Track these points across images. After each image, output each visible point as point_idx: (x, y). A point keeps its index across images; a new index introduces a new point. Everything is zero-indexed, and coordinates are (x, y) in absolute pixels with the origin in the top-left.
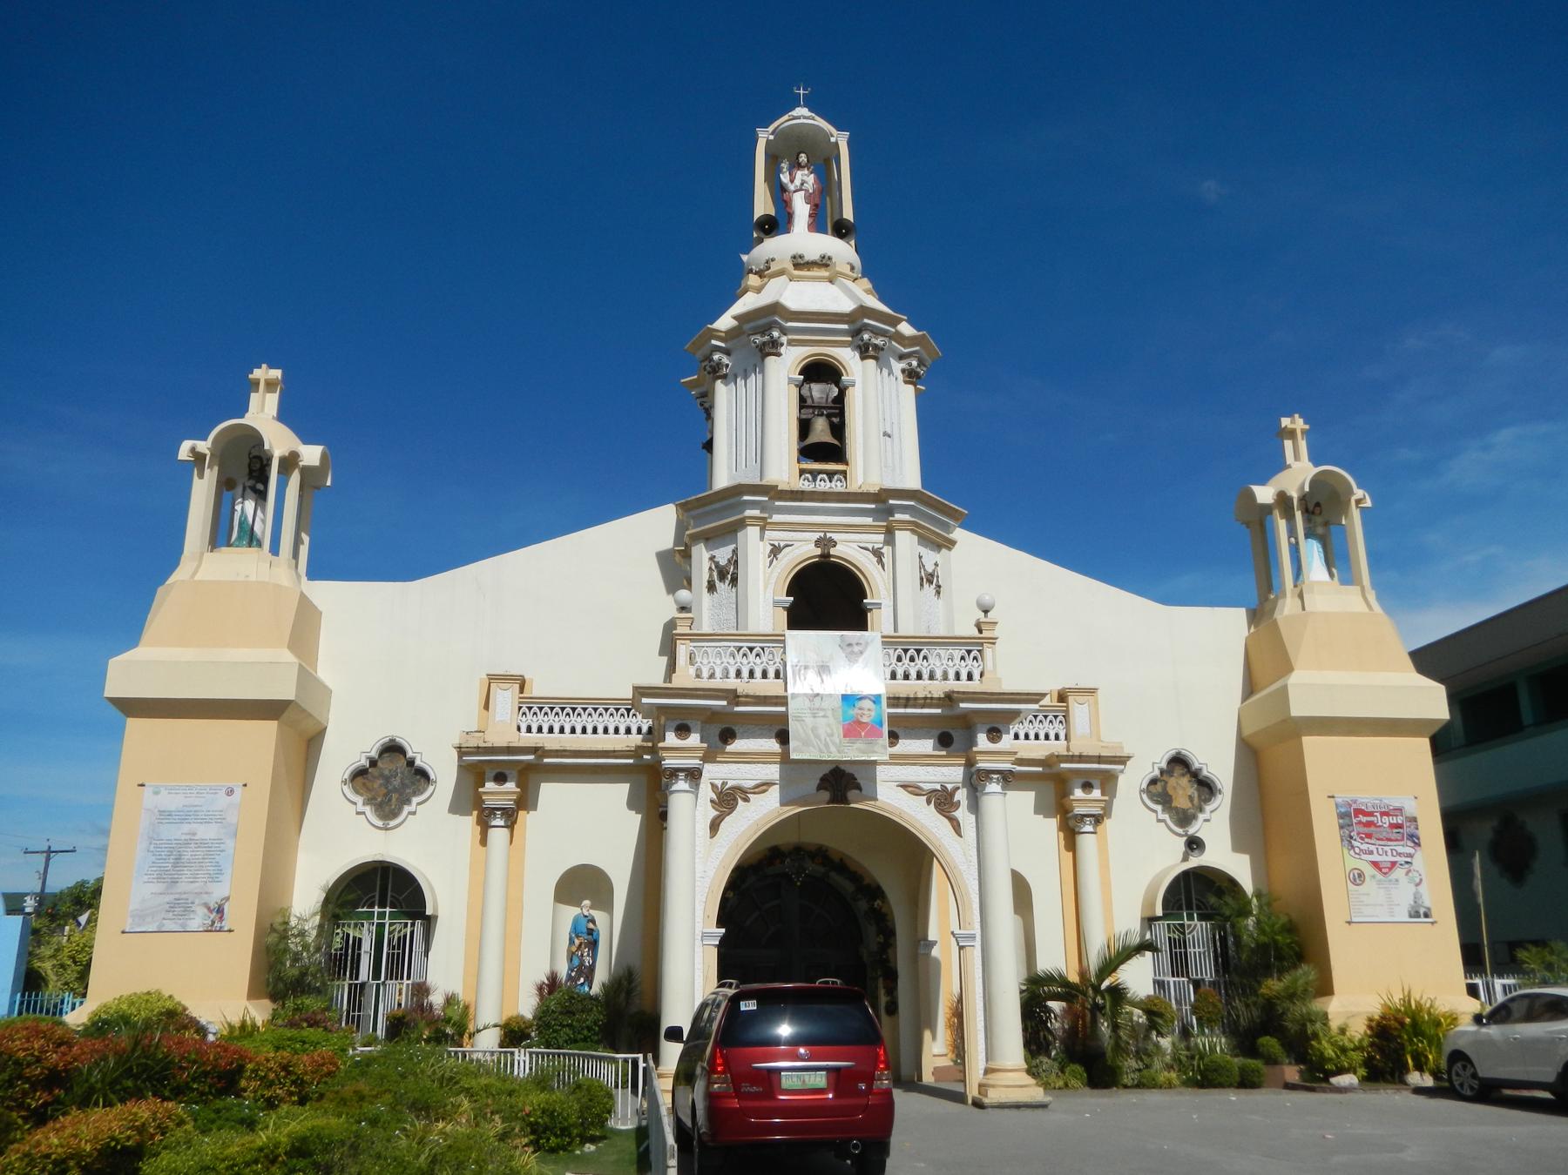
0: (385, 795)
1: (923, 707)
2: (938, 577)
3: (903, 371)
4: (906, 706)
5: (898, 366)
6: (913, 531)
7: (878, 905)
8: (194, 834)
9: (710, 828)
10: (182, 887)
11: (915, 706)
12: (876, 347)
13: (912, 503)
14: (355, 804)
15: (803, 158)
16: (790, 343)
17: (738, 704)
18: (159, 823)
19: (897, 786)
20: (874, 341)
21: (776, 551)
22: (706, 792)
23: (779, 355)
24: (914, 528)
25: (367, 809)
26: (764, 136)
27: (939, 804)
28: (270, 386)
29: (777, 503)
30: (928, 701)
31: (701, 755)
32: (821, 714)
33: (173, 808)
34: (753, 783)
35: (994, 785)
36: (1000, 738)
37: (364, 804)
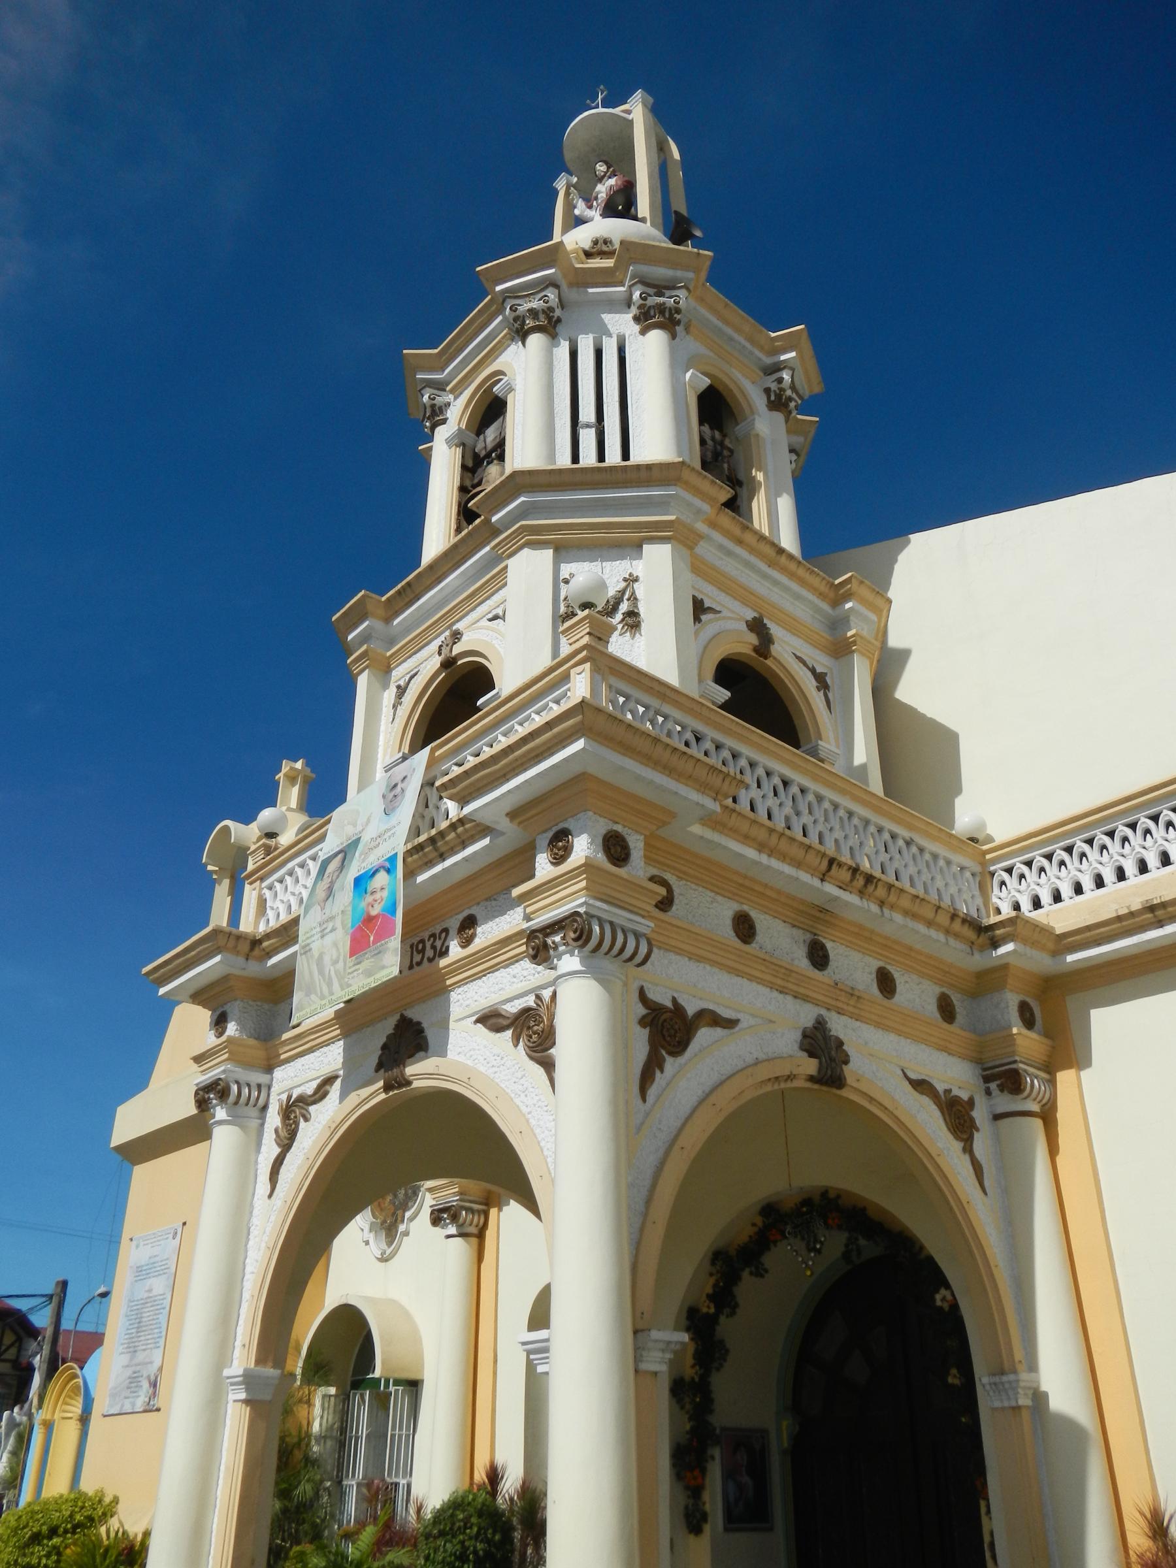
0: (394, 1214)
1: (464, 845)
2: (634, 599)
3: (637, 319)
4: (442, 857)
5: (622, 323)
6: (532, 545)
7: (944, 1299)
8: (150, 1291)
9: (270, 1179)
10: (141, 1357)
11: (453, 851)
12: (533, 313)
13: (522, 499)
14: (362, 1230)
15: (601, 168)
16: (457, 391)
17: (269, 954)
18: (136, 1281)
19: (478, 1021)
20: (525, 306)
21: (401, 691)
22: (273, 1119)
23: (444, 421)
24: (535, 539)
25: (371, 1237)
26: (561, 184)
27: (531, 1037)
28: (292, 780)
29: (395, 622)
30: (460, 830)
31: (226, 1056)
32: (330, 925)
33: (143, 1263)
34: (314, 1085)
35: (566, 957)
36: (568, 850)
37: (370, 1231)
